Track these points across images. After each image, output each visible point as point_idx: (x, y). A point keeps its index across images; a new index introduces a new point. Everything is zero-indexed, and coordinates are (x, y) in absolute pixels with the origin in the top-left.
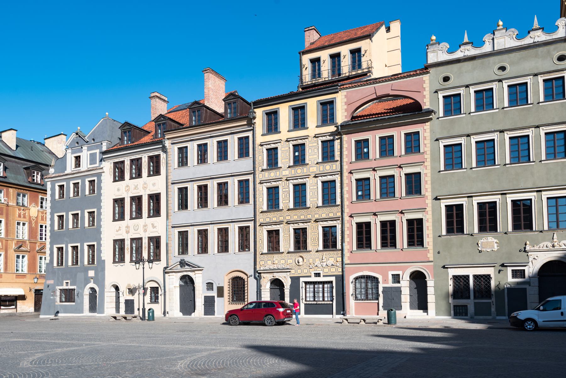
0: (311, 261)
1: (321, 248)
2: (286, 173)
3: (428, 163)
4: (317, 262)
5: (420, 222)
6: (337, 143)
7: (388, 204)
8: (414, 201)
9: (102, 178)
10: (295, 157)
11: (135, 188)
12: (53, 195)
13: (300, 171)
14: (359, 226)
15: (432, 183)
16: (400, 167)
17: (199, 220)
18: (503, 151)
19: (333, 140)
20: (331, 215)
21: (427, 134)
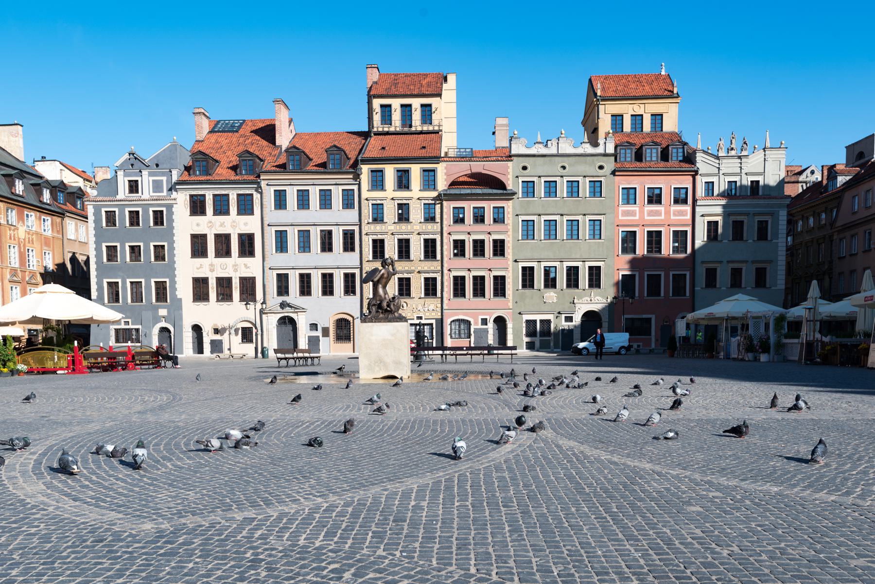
0: (414, 306)
1: (423, 295)
2: (392, 228)
3: (510, 233)
4: (420, 308)
5: (503, 278)
6: (438, 207)
7: (479, 262)
8: (498, 261)
9: (174, 210)
10: (399, 214)
11: (221, 226)
12: (97, 221)
13: (404, 227)
14: (456, 278)
15: (513, 249)
16: (489, 233)
17: (301, 264)
18: (563, 231)
19: (435, 204)
20: (432, 268)
21: (510, 210)
